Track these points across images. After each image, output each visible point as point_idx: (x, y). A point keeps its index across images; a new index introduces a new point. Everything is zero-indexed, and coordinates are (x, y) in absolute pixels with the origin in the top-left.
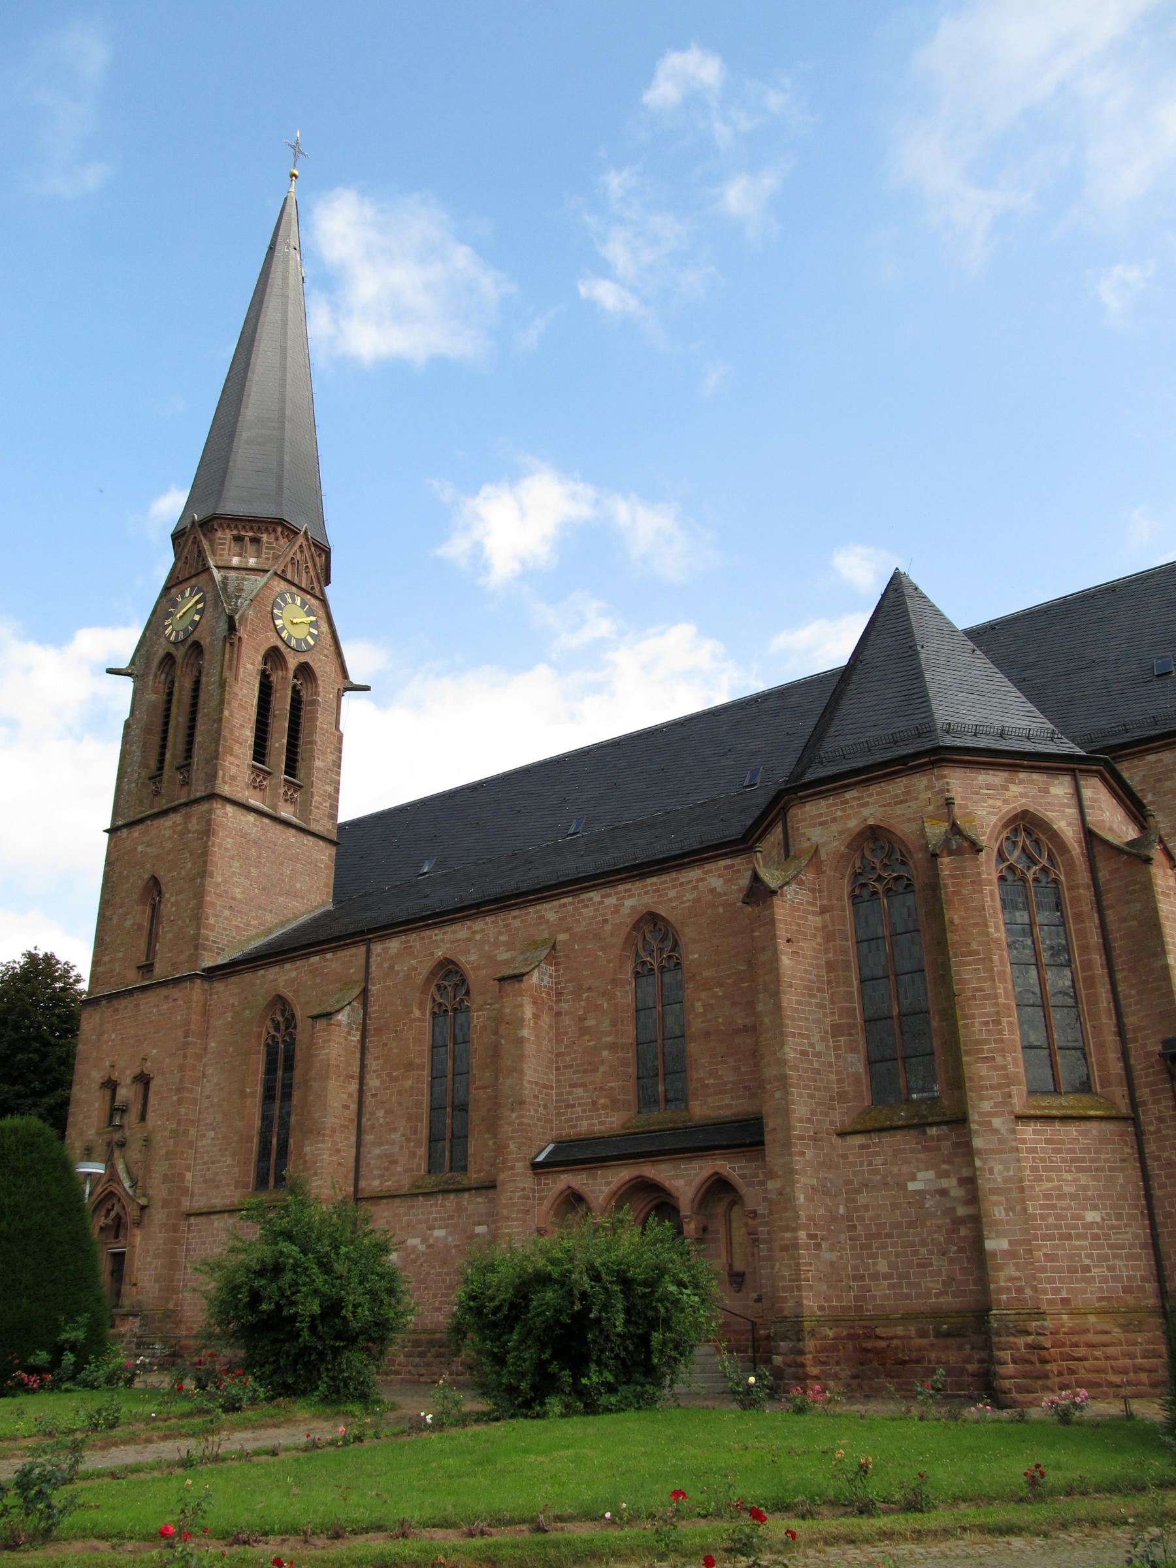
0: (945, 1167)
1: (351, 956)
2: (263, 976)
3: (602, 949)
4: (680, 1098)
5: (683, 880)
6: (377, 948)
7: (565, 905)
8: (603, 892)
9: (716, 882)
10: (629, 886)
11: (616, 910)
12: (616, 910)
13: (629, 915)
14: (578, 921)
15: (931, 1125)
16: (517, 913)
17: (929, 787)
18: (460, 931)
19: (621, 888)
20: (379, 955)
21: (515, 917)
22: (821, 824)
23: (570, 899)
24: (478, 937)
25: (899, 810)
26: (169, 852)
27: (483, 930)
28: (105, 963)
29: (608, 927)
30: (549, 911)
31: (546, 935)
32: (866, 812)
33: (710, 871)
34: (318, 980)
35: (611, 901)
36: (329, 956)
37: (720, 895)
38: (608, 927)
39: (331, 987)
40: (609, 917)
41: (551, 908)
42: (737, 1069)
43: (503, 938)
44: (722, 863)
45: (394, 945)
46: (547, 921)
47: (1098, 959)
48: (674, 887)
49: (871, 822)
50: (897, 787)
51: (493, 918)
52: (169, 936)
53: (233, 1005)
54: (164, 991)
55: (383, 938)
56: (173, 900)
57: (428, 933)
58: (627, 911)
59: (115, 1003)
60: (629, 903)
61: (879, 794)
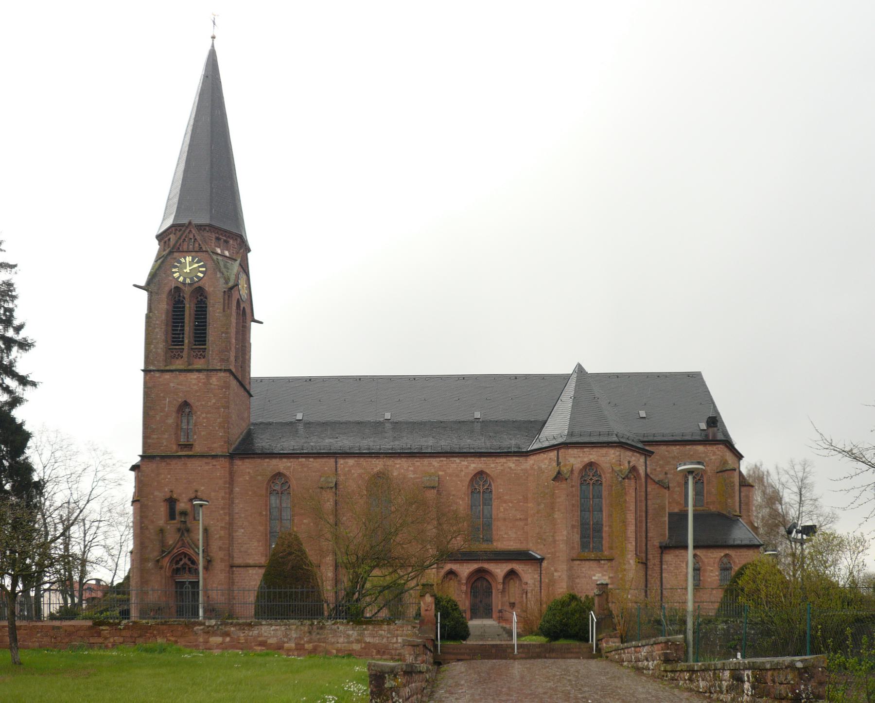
0: (605, 573)
1: (325, 462)
2: (269, 462)
3: (460, 481)
4: (489, 540)
5: (498, 462)
6: (341, 461)
7: (442, 461)
8: (461, 459)
9: (512, 465)
10: (473, 459)
11: (467, 467)
12: (467, 467)
13: (473, 470)
14: (449, 468)
15: (602, 560)
16: (418, 459)
17: (614, 454)
18: (390, 462)
19: (469, 459)
20: (341, 464)
21: (417, 461)
22: (574, 457)
23: (445, 459)
24: (398, 466)
25: (603, 459)
26: (196, 391)
27: (400, 464)
28: (154, 438)
29: (463, 473)
30: (435, 462)
31: (433, 471)
32: (591, 457)
33: (510, 460)
34: (305, 469)
35: (465, 463)
36: (311, 460)
37: (513, 470)
38: (463, 473)
39: (314, 474)
40: (464, 469)
41: (436, 461)
42: (516, 533)
43: (411, 469)
44: (515, 458)
45: (351, 462)
46: (434, 466)
47: (644, 514)
48: (493, 463)
49: (593, 460)
50: (604, 451)
51: (406, 459)
52: (203, 433)
53: (249, 473)
54: (205, 460)
55: (343, 457)
56: (204, 415)
57: (370, 459)
58: (472, 468)
59: (168, 461)
60: (473, 466)
61: (596, 452)
